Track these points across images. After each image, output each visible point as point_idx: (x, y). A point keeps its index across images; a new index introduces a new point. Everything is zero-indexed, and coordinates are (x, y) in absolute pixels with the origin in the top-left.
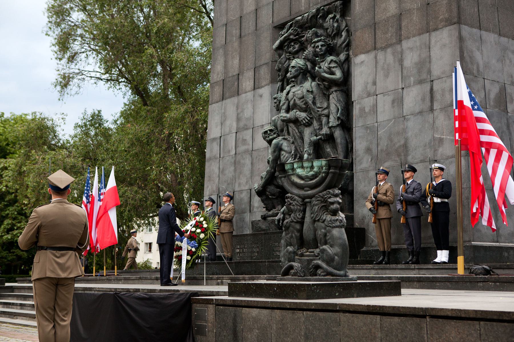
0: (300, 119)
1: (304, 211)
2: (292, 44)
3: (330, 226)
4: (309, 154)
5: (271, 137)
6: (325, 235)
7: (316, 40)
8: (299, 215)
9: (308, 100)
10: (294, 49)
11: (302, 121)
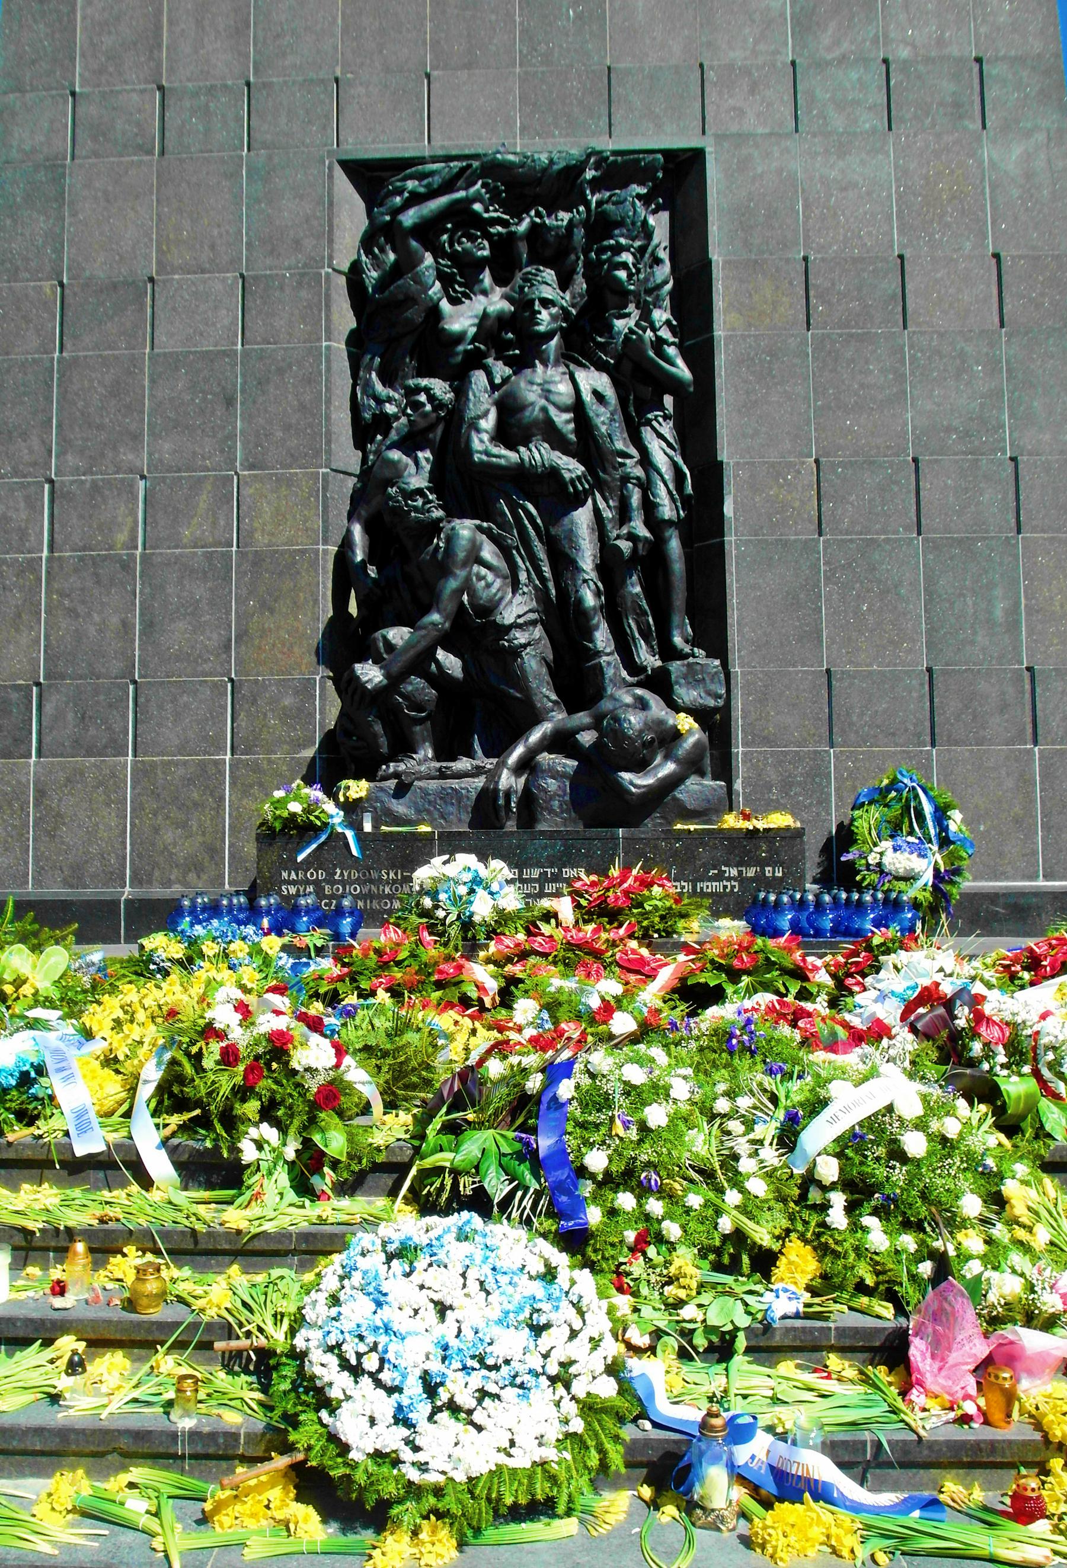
0: (567, 476)
4: (598, 594)
11: (572, 481)
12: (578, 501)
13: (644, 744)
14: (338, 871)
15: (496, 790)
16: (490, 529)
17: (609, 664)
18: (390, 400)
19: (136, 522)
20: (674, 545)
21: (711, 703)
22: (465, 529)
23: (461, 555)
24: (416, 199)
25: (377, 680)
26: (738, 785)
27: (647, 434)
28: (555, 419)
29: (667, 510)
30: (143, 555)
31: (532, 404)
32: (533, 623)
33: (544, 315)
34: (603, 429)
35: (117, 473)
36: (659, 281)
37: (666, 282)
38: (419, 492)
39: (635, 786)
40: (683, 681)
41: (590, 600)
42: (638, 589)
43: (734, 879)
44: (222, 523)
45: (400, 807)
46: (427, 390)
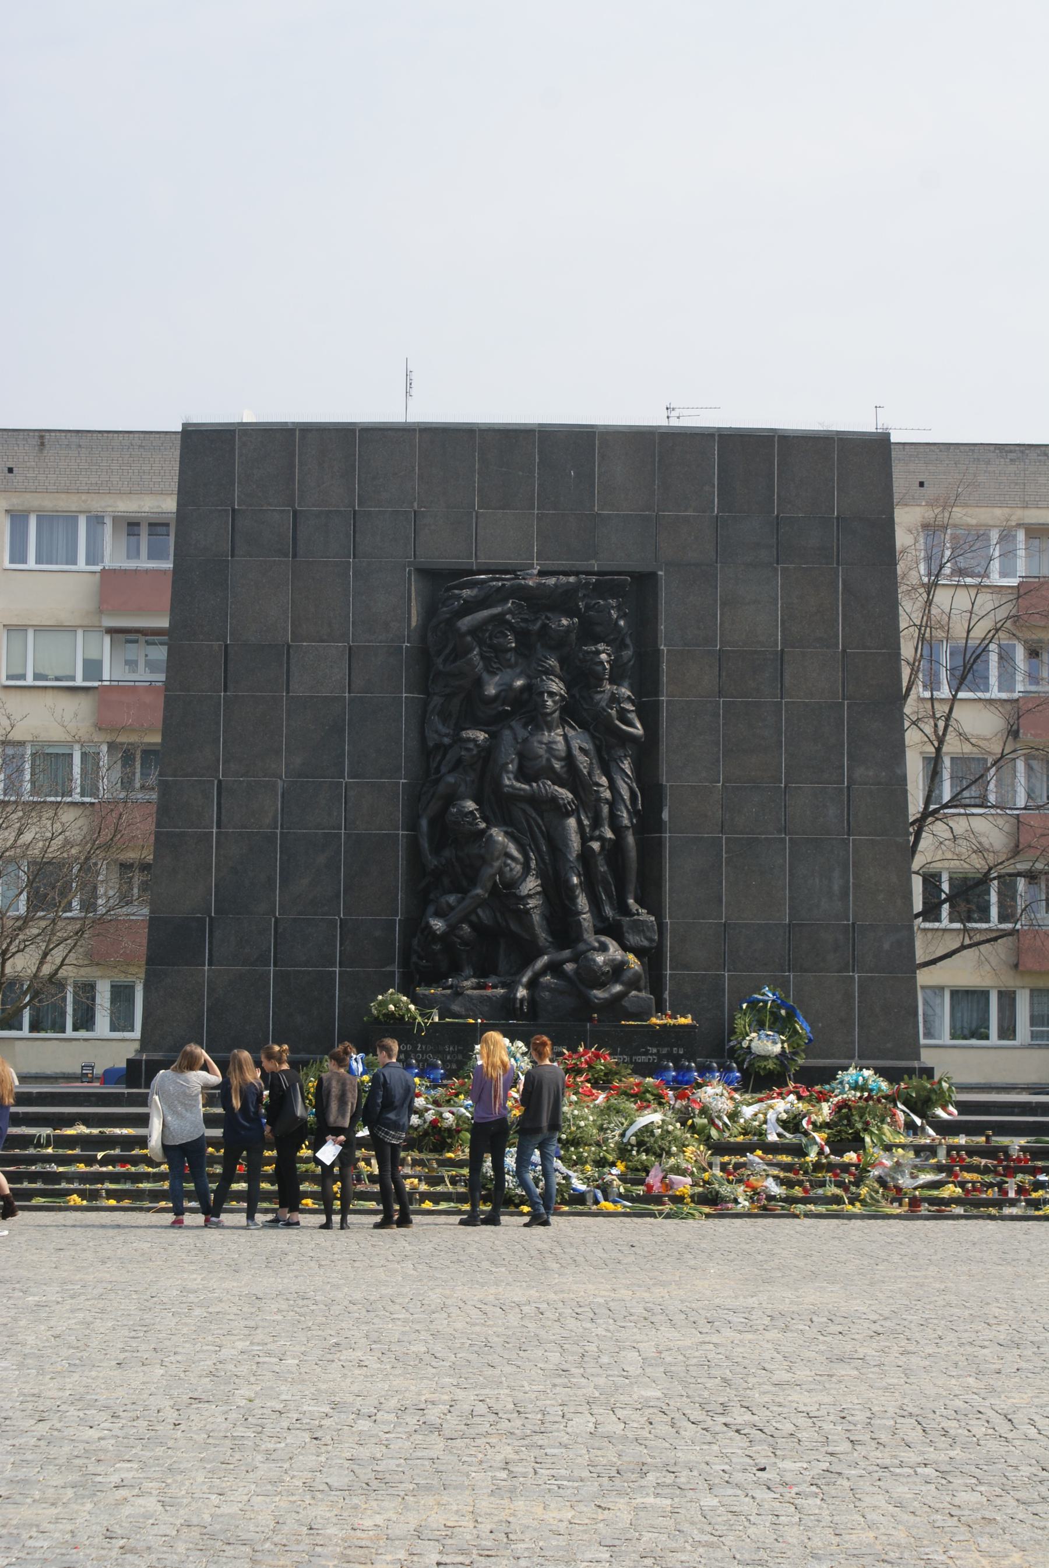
0: (561, 802)
4: (579, 876)
11: (565, 805)
12: (568, 815)
13: (603, 974)
14: (419, 1045)
15: (515, 998)
16: (513, 832)
17: (584, 919)
18: (446, 735)
19: (277, 810)
20: (631, 839)
21: (646, 943)
22: (498, 835)
23: (496, 854)
24: (470, 608)
25: (442, 929)
26: (666, 995)
27: (614, 769)
28: (556, 766)
29: (625, 819)
30: (281, 833)
31: (541, 756)
33: (550, 703)
34: (585, 771)
35: (264, 777)
36: (625, 661)
37: (629, 661)
38: (472, 812)
39: (597, 998)
40: (630, 931)
41: (575, 880)
42: (606, 868)
43: (655, 1054)
44: (335, 814)
45: (456, 1008)
46: (475, 740)
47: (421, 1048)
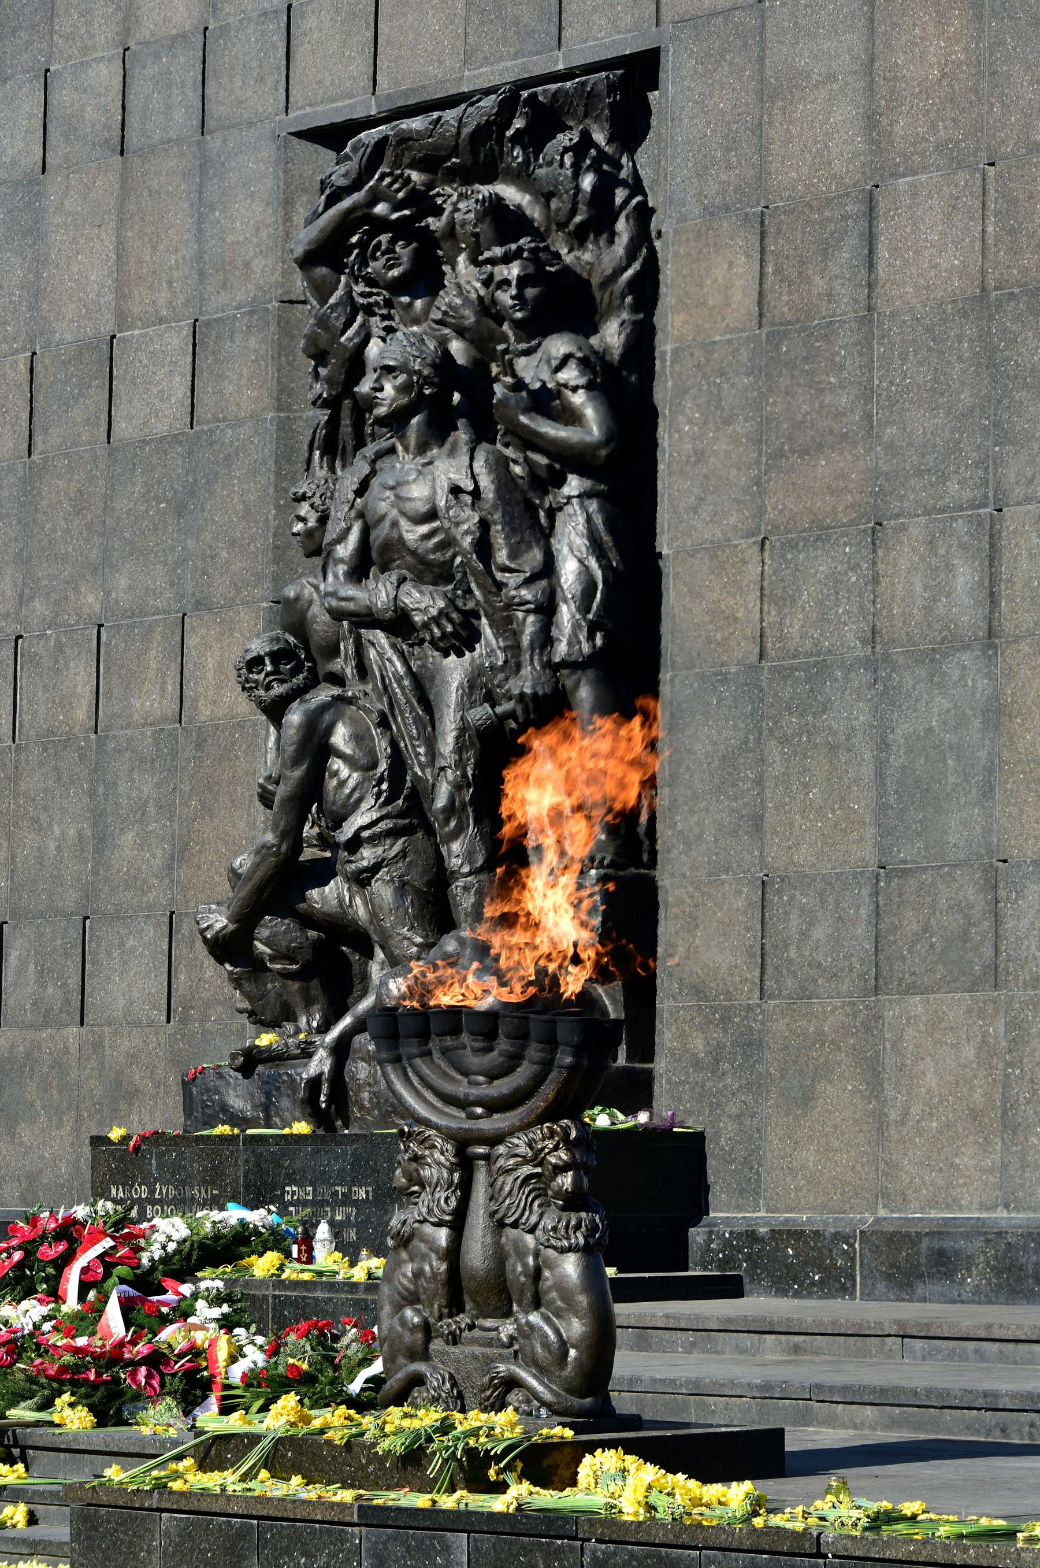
1: (466, 1188)
2: (384, 238)
3: (554, 1248)
5: (278, 689)
6: (537, 1275)
7: (498, 251)
8: (447, 1199)
9: (457, 532)
10: (392, 267)
11: (426, 626)
25: (218, 926)
31: (382, 518)
32: (393, 834)
47: (161, 1193)
